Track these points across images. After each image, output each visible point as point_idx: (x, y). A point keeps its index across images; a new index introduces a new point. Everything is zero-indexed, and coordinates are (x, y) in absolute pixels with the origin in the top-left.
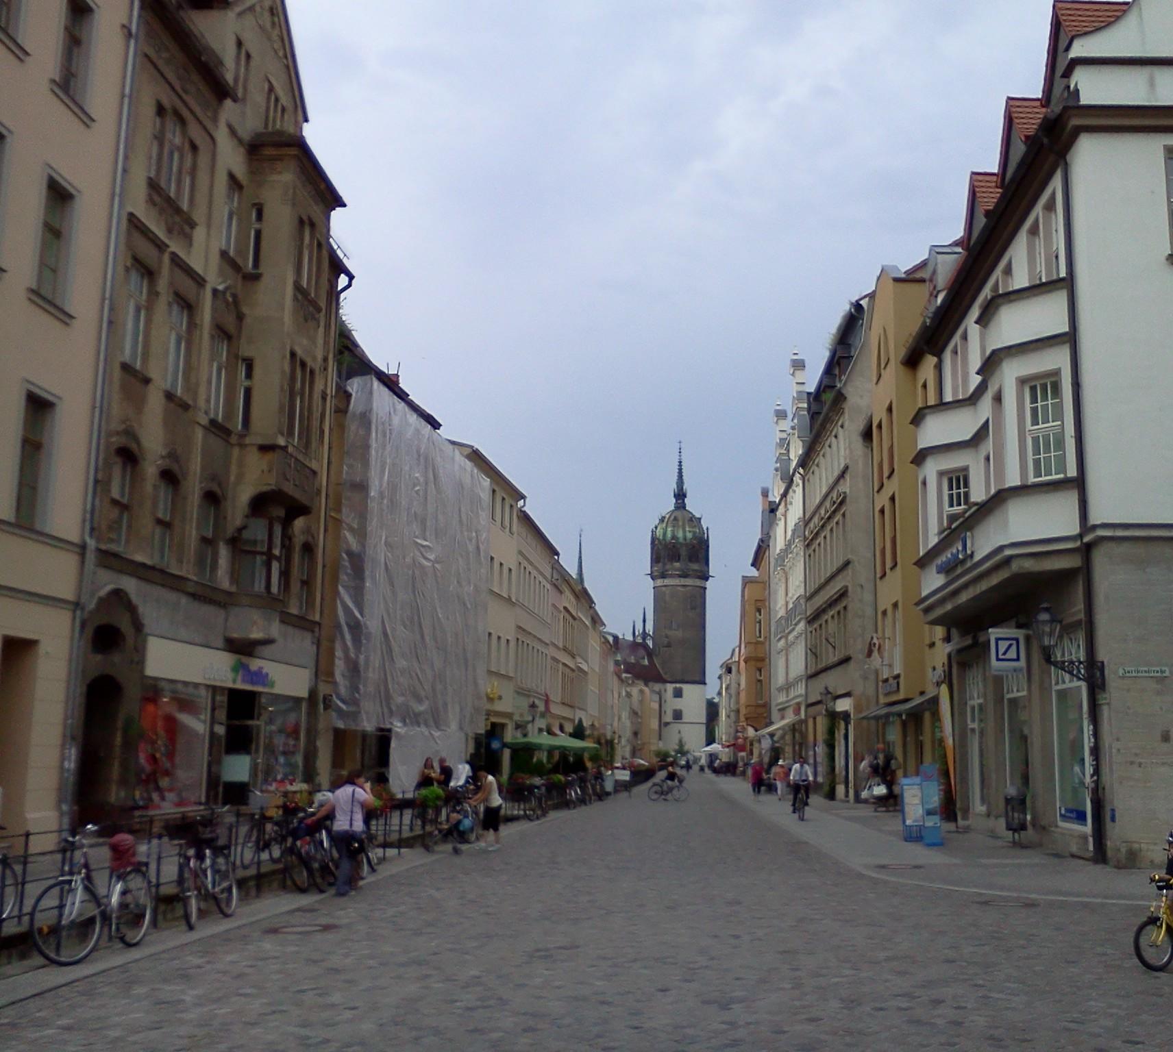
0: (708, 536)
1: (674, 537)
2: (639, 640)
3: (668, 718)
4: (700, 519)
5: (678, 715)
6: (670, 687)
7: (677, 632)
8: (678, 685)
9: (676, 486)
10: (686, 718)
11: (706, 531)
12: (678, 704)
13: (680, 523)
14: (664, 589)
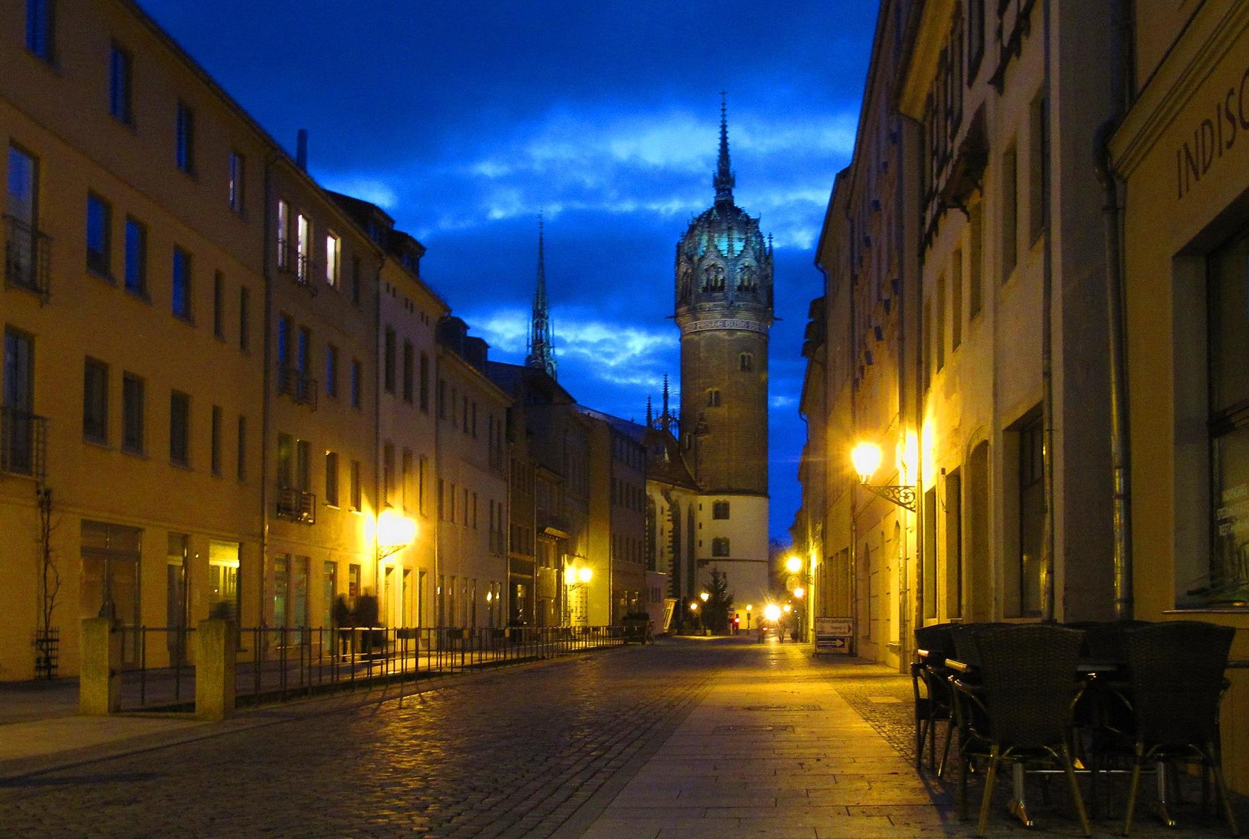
3: (705, 551)
5: (720, 547)
6: (707, 502)
8: (721, 498)
10: (734, 554)
12: (721, 528)
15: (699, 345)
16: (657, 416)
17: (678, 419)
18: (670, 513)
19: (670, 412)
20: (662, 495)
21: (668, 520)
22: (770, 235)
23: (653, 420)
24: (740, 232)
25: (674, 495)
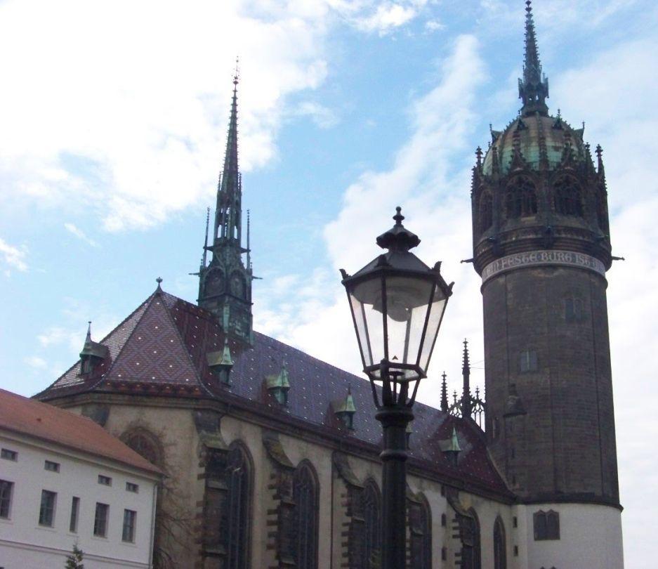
1: (517, 159)
2: (457, 412)
4: (581, 132)
6: (525, 514)
8: (546, 508)
9: (521, 76)
11: (596, 165)
13: (533, 133)
14: (501, 280)
15: (506, 288)
16: (455, 400)
17: (484, 401)
18: (457, 524)
19: (473, 394)
20: (443, 494)
21: (454, 537)
23: (449, 407)
24: (554, 139)
25: (466, 501)
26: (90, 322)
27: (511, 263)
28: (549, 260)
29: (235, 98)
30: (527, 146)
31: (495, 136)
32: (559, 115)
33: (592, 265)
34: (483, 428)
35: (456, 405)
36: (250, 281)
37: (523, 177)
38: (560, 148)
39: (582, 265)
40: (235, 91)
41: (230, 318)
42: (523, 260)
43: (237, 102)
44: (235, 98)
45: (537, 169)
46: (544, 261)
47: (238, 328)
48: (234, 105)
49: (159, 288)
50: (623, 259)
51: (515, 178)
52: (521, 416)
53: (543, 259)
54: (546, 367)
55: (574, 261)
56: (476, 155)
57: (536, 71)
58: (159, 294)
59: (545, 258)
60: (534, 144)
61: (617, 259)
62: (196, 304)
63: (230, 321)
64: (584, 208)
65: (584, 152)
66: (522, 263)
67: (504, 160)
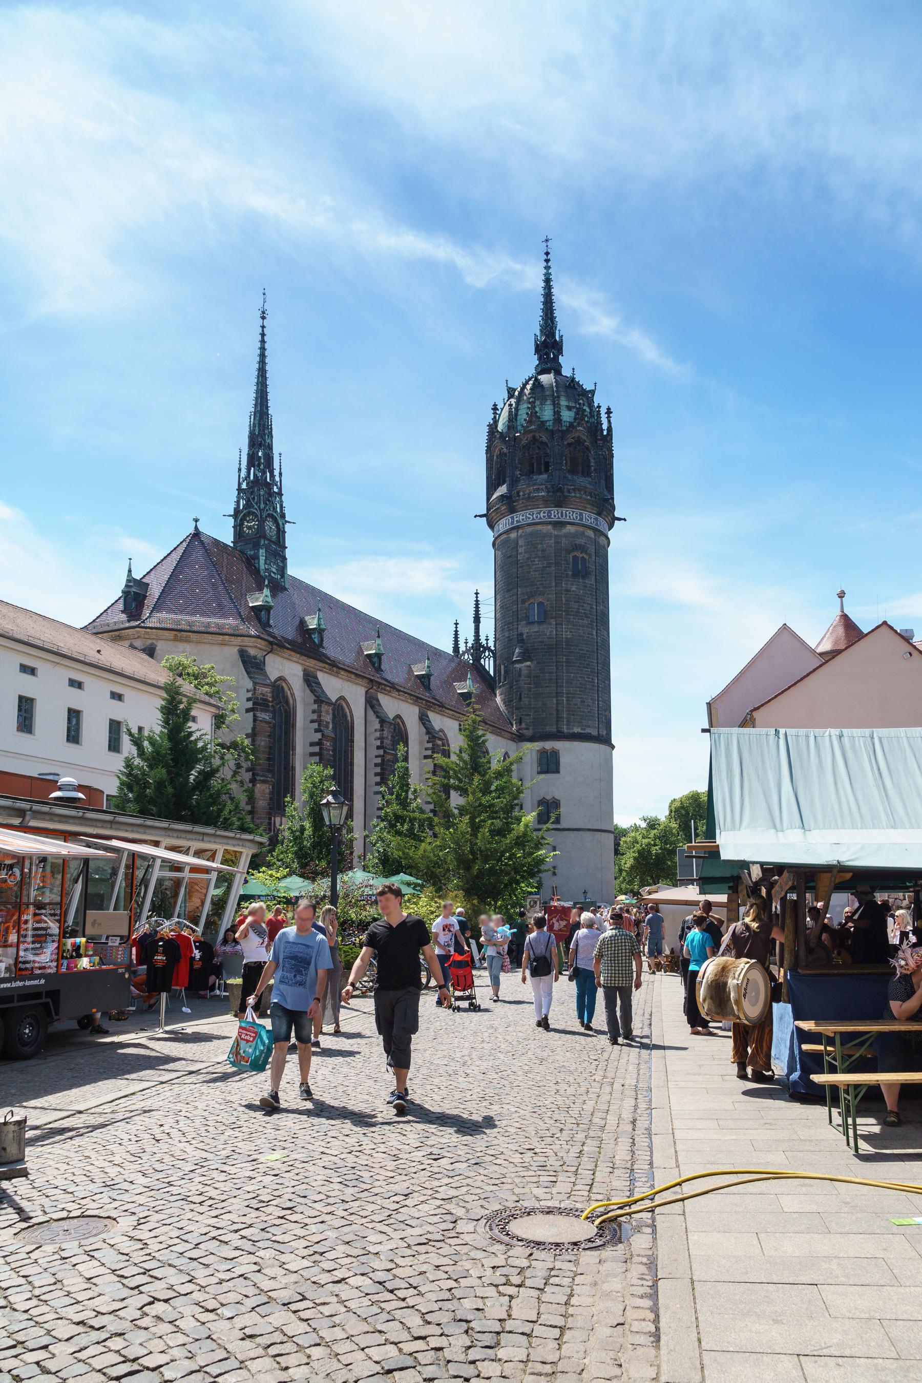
0: (610, 429)
1: (533, 416)
4: (593, 392)
6: (530, 749)
7: (543, 627)
8: (549, 745)
9: (538, 333)
11: (605, 426)
14: (513, 535)
15: (517, 544)
16: (466, 646)
17: (493, 648)
19: (483, 642)
22: (609, 409)
23: (461, 652)
24: (568, 400)
26: (130, 559)
27: (523, 519)
28: (558, 518)
29: (263, 335)
30: (541, 404)
31: (511, 392)
32: (573, 374)
33: (597, 524)
34: (492, 673)
35: (467, 651)
36: (283, 525)
37: (537, 435)
38: (574, 407)
39: (588, 523)
40: (263, 327)
41: (266, 559)
42: (535, 517)
43: (266, 338)
44: (263, 335)
45: (551, 428)
46: (554, 519)
47: (274, 570)
48: (263, 342)
49: (196, 527)
50: (625, 520)
51: (530, 435)
52: (528, 663)
53: (553, 516)
54: (552, 618)
55: (581, 519)
56: (492, 411)
57: (552, 328)
58: (197, 535)
59: (555, 516)
60: (548, 402)
61: (619, 519)
62: (232, 545)
63: (265, 563)
64: (593, 468)
65: (595, 414)
66: (533, 519)
67: (519, 417)
